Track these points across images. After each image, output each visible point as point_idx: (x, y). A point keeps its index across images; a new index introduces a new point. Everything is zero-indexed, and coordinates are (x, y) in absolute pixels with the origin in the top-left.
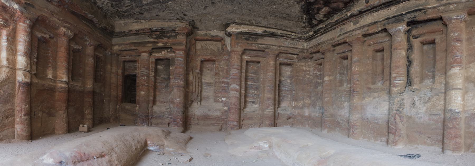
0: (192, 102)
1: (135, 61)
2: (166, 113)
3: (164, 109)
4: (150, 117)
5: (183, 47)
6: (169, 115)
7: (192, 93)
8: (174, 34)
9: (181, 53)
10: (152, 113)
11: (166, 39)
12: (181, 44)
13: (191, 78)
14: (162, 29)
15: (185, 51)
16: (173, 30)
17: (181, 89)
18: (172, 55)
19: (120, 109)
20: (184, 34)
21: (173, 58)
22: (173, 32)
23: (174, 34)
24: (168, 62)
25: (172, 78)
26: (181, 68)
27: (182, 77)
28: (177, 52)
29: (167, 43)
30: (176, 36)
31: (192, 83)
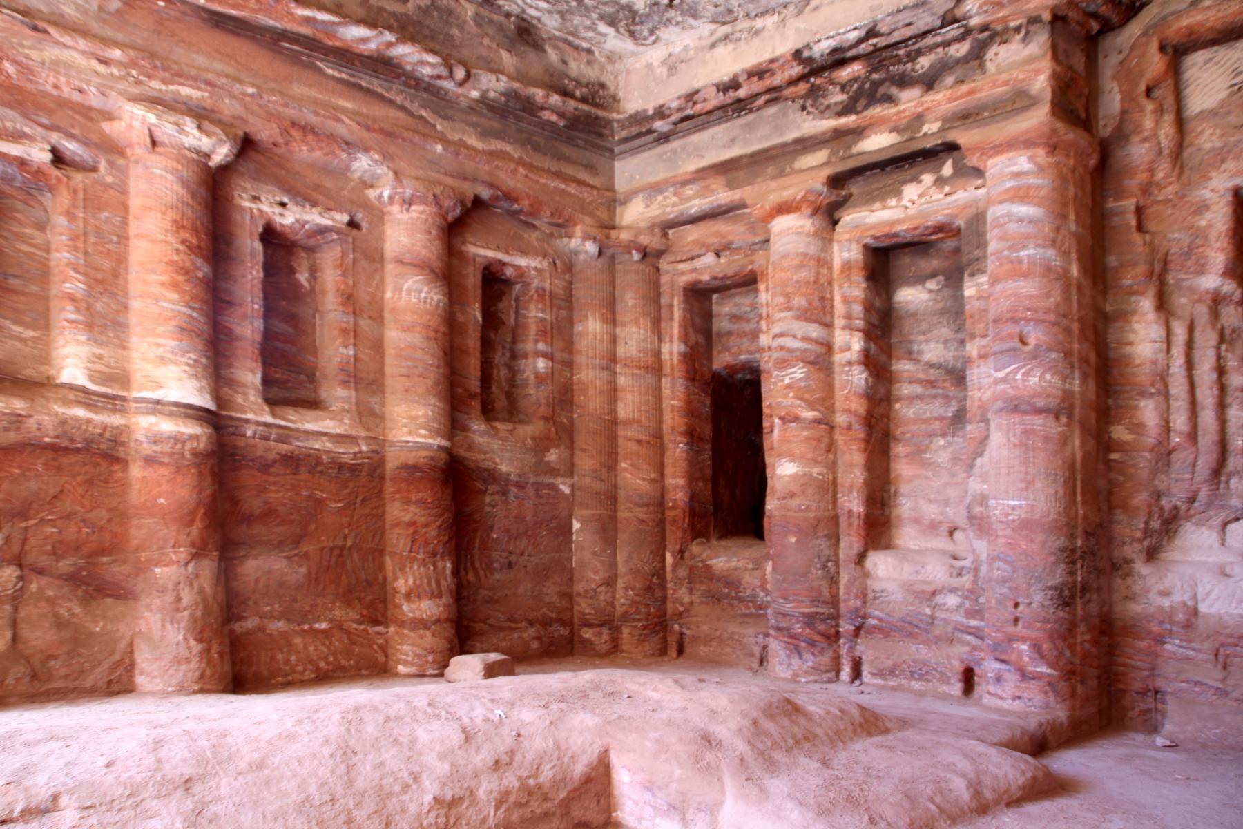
0: (1170, 523)
1: (749, 282)
2: (952, 600)
3: (936, 572)
4: (846, 627)
5: (1039, 117)
6: (971, 614)
7: (1164, 454)
8: (962, 49)
9: (1022, 162)
10: (863, 595)
11: (909, 100)
12: (1019, 100)
13: (1144, 338)
14: (872, 33)
15: (1053, 148)
16: (949, 19)
17: (1038, 422)
18: (966, 194)
19: (683, 572)
20: (1034, 20)
21: (978, 219)
22: (953, 31)
23: (962, 49)
24: (943, 250)
25: (983, 357)
26: (1025, 275)
27: (1036, 336)
28: (996, 166)
29: (918, 119)
30: (977, 55)
31: (1163, 377)
